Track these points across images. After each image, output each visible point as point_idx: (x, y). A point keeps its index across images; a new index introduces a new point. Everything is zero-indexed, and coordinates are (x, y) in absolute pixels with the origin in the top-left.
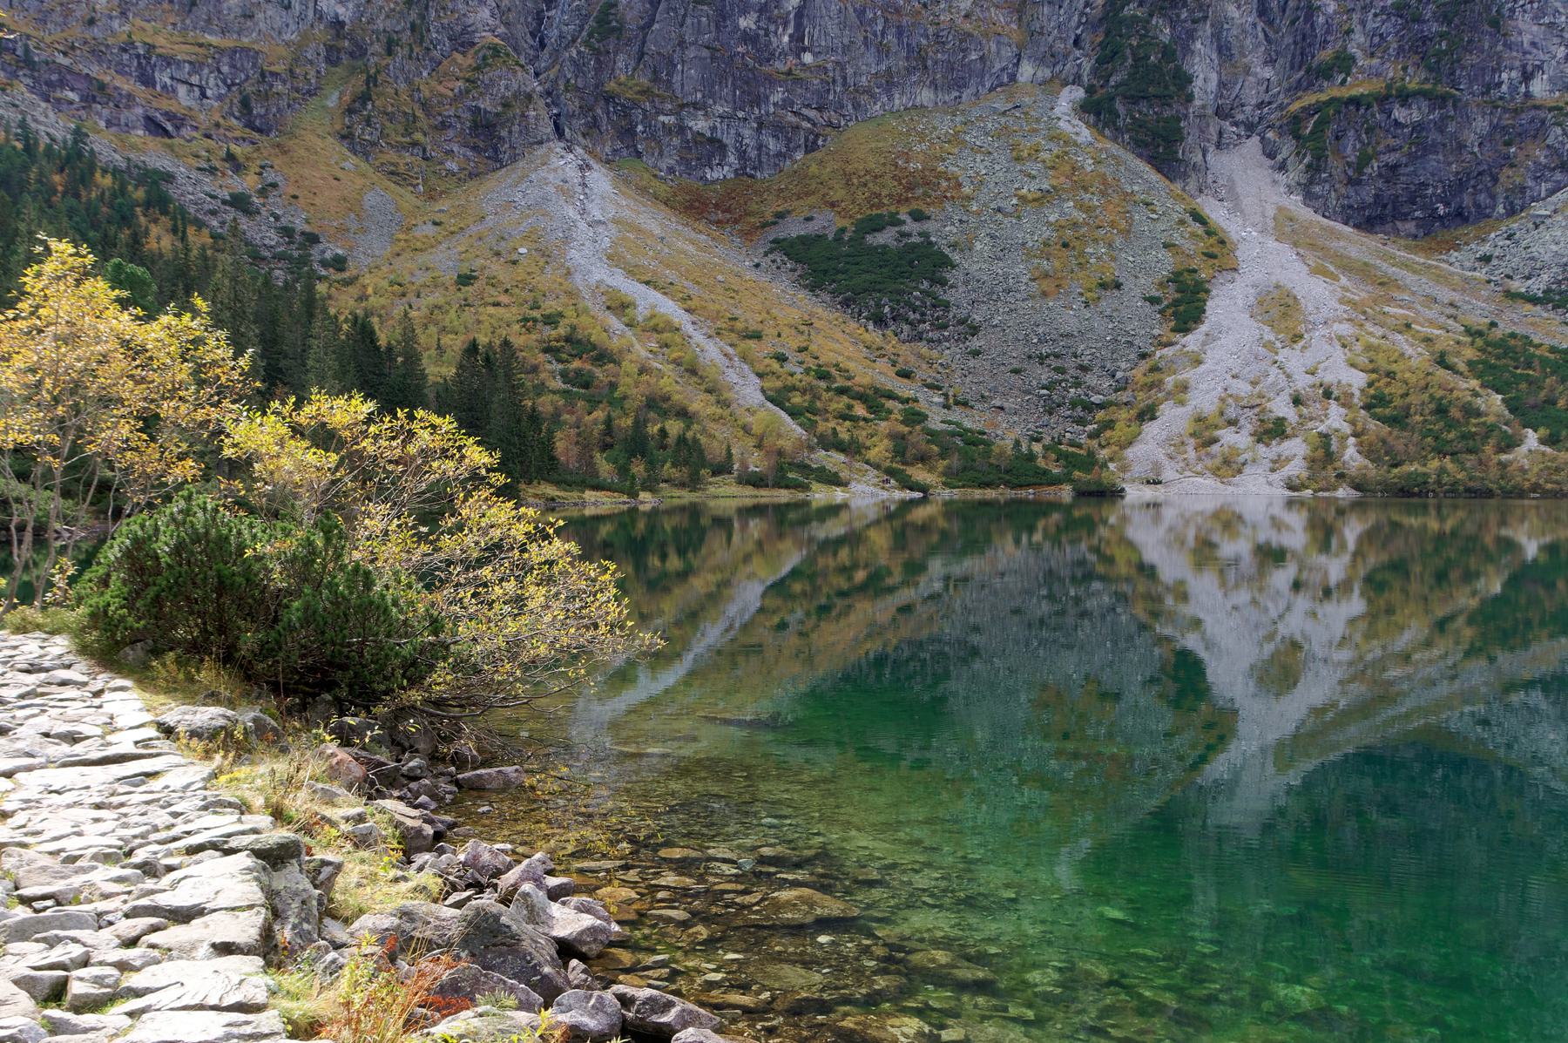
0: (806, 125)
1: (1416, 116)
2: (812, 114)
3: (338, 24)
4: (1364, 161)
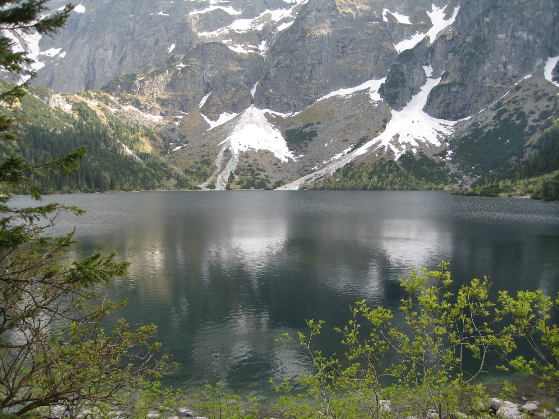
0: (310, 99)
1: (456, 90)
2: (311, 95)
3: (208, 84)
4: (442, 102)
